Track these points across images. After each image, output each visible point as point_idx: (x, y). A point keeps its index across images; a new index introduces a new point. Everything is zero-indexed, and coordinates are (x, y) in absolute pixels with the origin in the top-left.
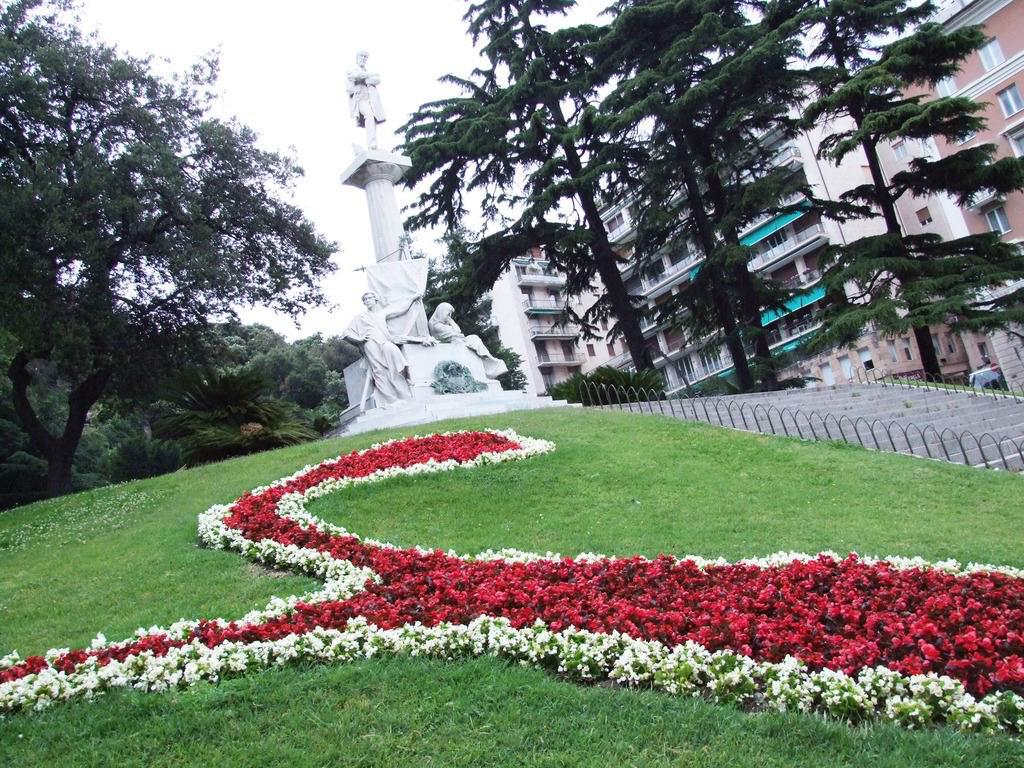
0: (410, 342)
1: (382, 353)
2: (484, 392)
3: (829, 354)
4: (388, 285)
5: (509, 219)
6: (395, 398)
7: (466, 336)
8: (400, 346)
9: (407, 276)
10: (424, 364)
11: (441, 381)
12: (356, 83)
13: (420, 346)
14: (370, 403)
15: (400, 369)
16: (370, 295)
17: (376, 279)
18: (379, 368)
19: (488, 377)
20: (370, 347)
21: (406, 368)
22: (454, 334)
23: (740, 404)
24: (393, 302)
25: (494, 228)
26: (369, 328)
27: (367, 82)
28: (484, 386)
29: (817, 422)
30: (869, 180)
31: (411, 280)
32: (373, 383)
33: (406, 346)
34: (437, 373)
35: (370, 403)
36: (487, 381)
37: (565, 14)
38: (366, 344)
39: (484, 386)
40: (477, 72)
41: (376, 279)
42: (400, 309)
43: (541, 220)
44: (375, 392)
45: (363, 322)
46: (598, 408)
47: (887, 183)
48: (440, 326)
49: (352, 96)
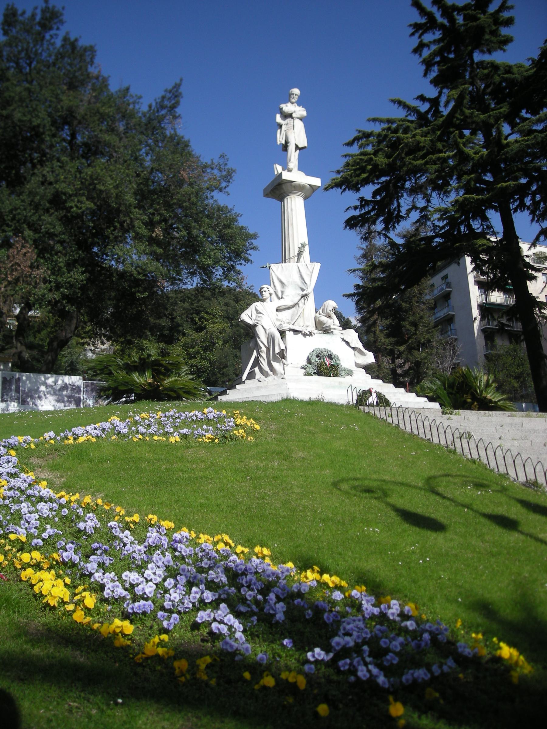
0: (290, 330)
2: (349, 377)
4: (284, 281)
6: (271, 373)
7: (344, 329)
14: (251, 376)
19: (357, 365)
26: (260, 315)
28: (350, 373)
33: (287, 332)
35: (251, 376)
36: (353, 368)
37: (504, 51)
38: (257, 329)
39: (350, 373)
40: (422, 98)
44: (257, 369)
45: (256, 310)
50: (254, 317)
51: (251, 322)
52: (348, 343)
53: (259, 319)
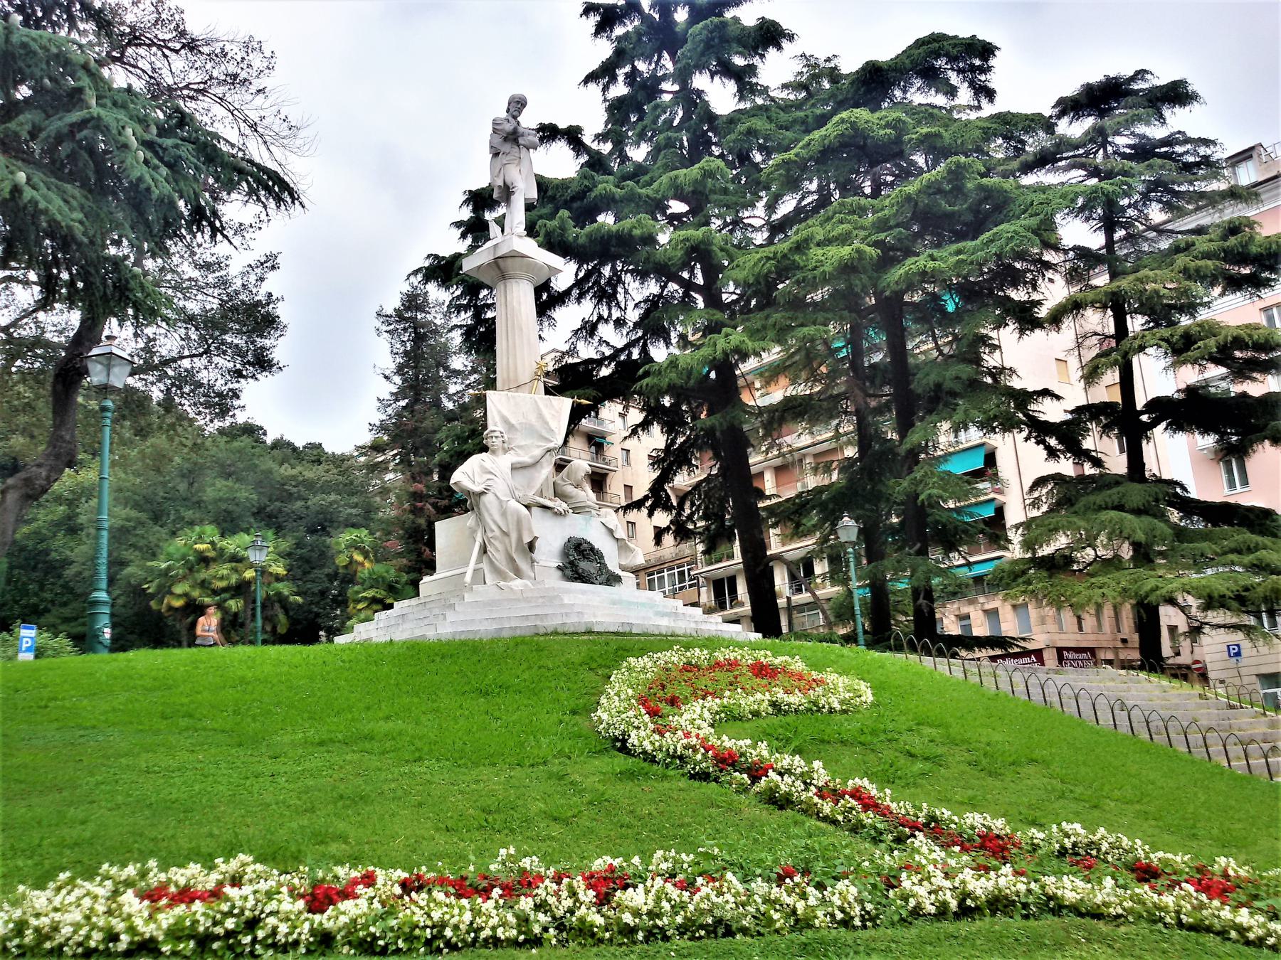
1: (504, 514)
3: (972, 602)
4: (513, 421)
5: (608, 344)
6: (512, 575)
8: (528, 507)
9: (541, 416)
10: (551, 537)
11: (572, 563)
12: (506, 139)
13: (549, 513)
15: (527, 539)
16: (497, 434)
17: (499, 412)
18: (497, 532)
20: (488, 500)
21: (536, 538)
22: (589, 503)
23: (1060, 684)
24: (520, 447)
25: (587, 351)
27: (521, 141)
29: (1156, 724)
30: (1116, 396)
31: (546, 423)
32: (484, 550)
33: (534, 509)
34: (565, 553)
36: (619, 572)
38: (485, 499)
41: (499, 412)
42: (526, 459)
43: (644, 351)
46: (913, 657)
47: (1140, 403)
48: (570, 489)
49: (496, 155)
50: (477, 479)
51: (477, 488)
52: (611, 532)
53: (489, 483)
